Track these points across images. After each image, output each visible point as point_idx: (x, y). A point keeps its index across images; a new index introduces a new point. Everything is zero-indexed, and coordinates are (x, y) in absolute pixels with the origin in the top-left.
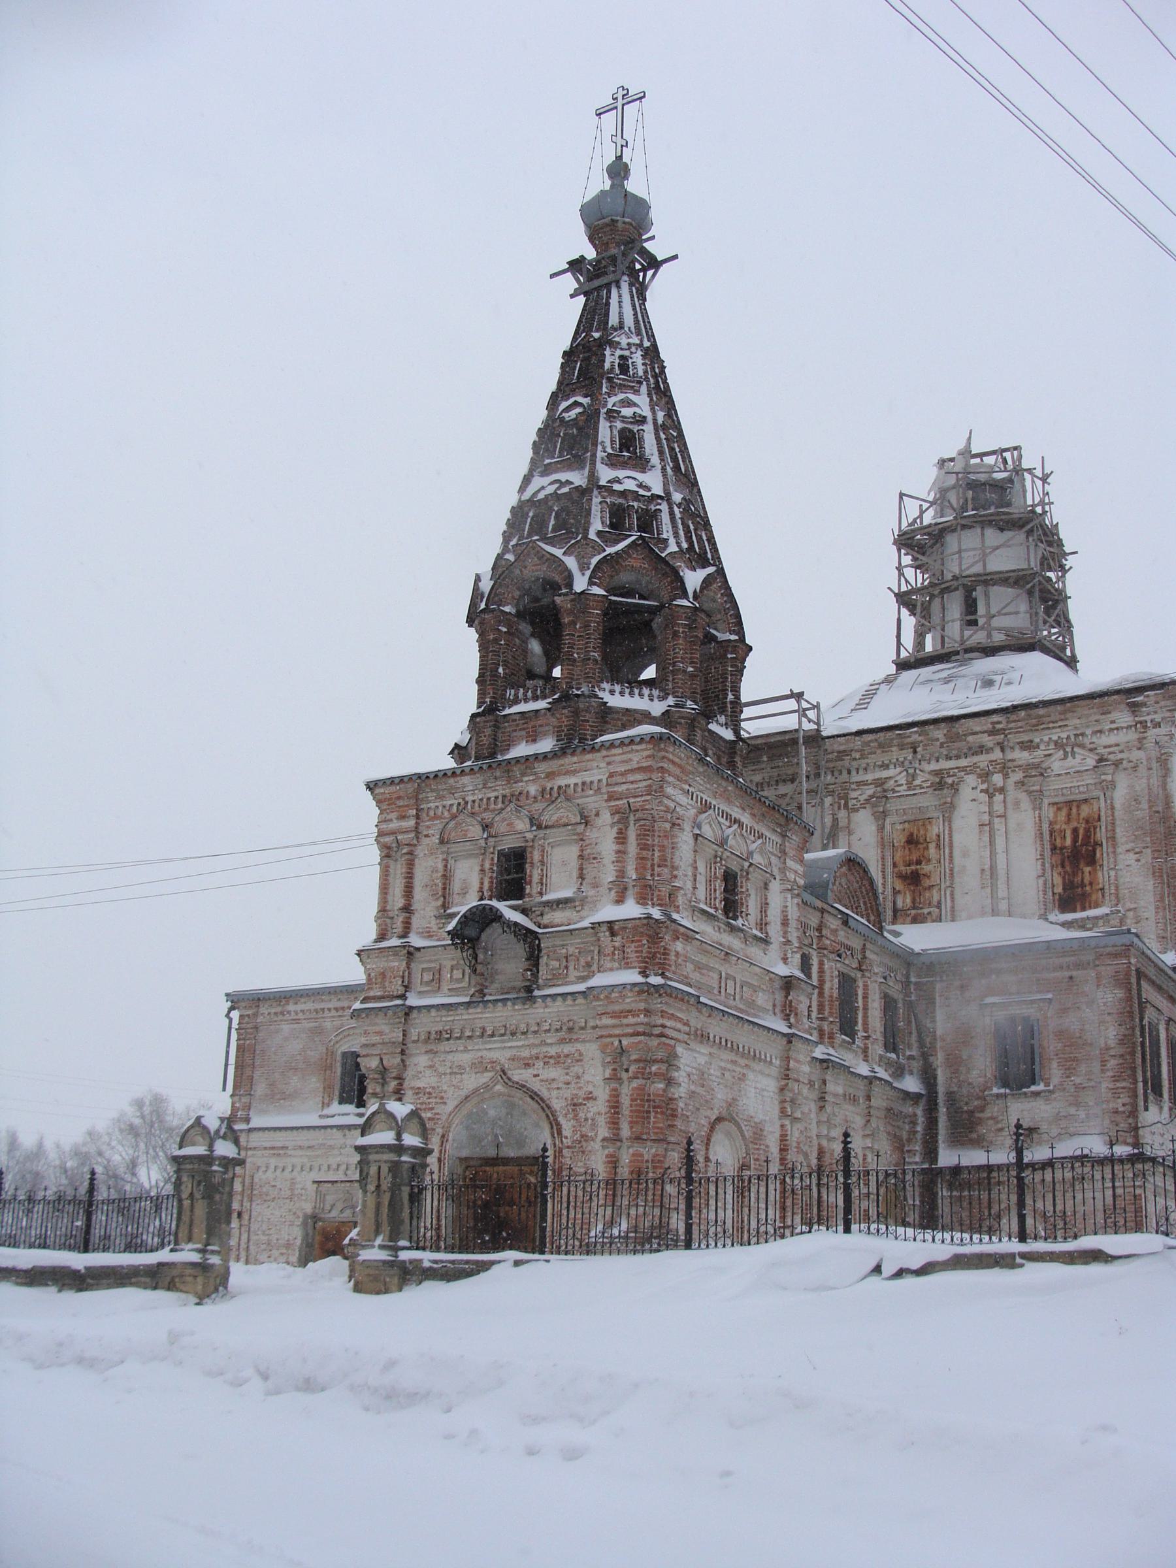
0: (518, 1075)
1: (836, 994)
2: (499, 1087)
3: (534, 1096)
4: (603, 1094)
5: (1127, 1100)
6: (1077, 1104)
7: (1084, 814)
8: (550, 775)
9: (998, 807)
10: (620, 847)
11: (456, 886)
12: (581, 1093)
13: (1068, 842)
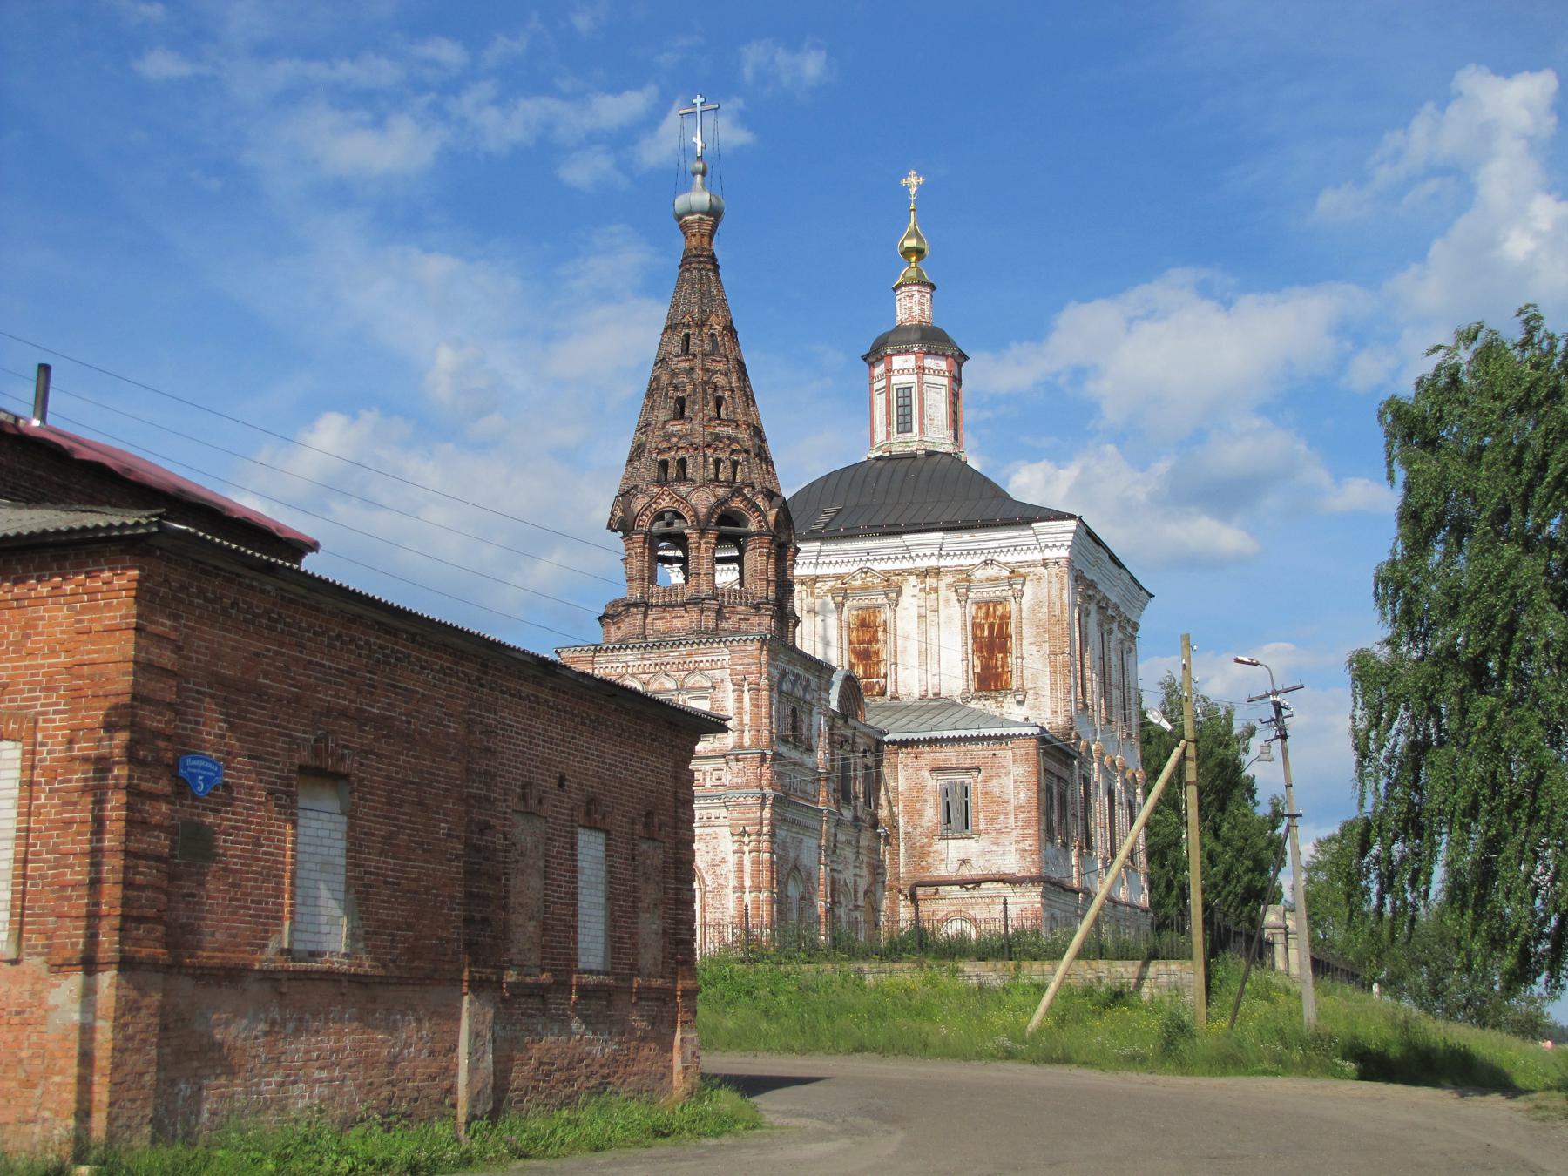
4: (732, 860)
6: (996, 843)
8: (690, 655)
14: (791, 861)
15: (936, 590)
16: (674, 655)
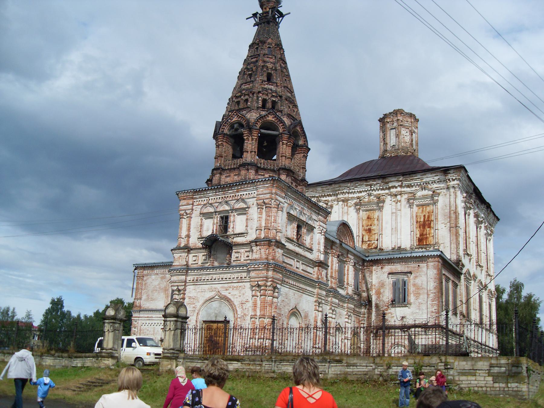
0: (224, 293)
1: (337, 268)
2: (217, 297)
3: (228, 300)
5: (436, 308)
6: (419, 309)
7: (427, 210)
9: (399, 207)
10: (260, 216)
11: (205, 228)
12: (245, 300)
13: (422, 220)
14: (292, 306)
15: (400, 201)
16: (230, 193)
